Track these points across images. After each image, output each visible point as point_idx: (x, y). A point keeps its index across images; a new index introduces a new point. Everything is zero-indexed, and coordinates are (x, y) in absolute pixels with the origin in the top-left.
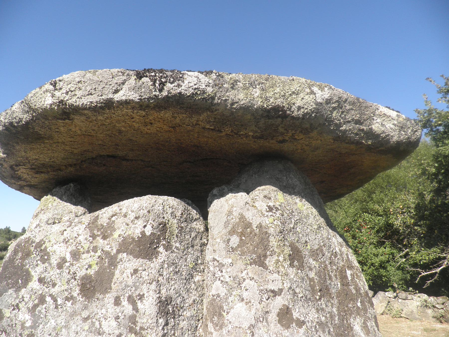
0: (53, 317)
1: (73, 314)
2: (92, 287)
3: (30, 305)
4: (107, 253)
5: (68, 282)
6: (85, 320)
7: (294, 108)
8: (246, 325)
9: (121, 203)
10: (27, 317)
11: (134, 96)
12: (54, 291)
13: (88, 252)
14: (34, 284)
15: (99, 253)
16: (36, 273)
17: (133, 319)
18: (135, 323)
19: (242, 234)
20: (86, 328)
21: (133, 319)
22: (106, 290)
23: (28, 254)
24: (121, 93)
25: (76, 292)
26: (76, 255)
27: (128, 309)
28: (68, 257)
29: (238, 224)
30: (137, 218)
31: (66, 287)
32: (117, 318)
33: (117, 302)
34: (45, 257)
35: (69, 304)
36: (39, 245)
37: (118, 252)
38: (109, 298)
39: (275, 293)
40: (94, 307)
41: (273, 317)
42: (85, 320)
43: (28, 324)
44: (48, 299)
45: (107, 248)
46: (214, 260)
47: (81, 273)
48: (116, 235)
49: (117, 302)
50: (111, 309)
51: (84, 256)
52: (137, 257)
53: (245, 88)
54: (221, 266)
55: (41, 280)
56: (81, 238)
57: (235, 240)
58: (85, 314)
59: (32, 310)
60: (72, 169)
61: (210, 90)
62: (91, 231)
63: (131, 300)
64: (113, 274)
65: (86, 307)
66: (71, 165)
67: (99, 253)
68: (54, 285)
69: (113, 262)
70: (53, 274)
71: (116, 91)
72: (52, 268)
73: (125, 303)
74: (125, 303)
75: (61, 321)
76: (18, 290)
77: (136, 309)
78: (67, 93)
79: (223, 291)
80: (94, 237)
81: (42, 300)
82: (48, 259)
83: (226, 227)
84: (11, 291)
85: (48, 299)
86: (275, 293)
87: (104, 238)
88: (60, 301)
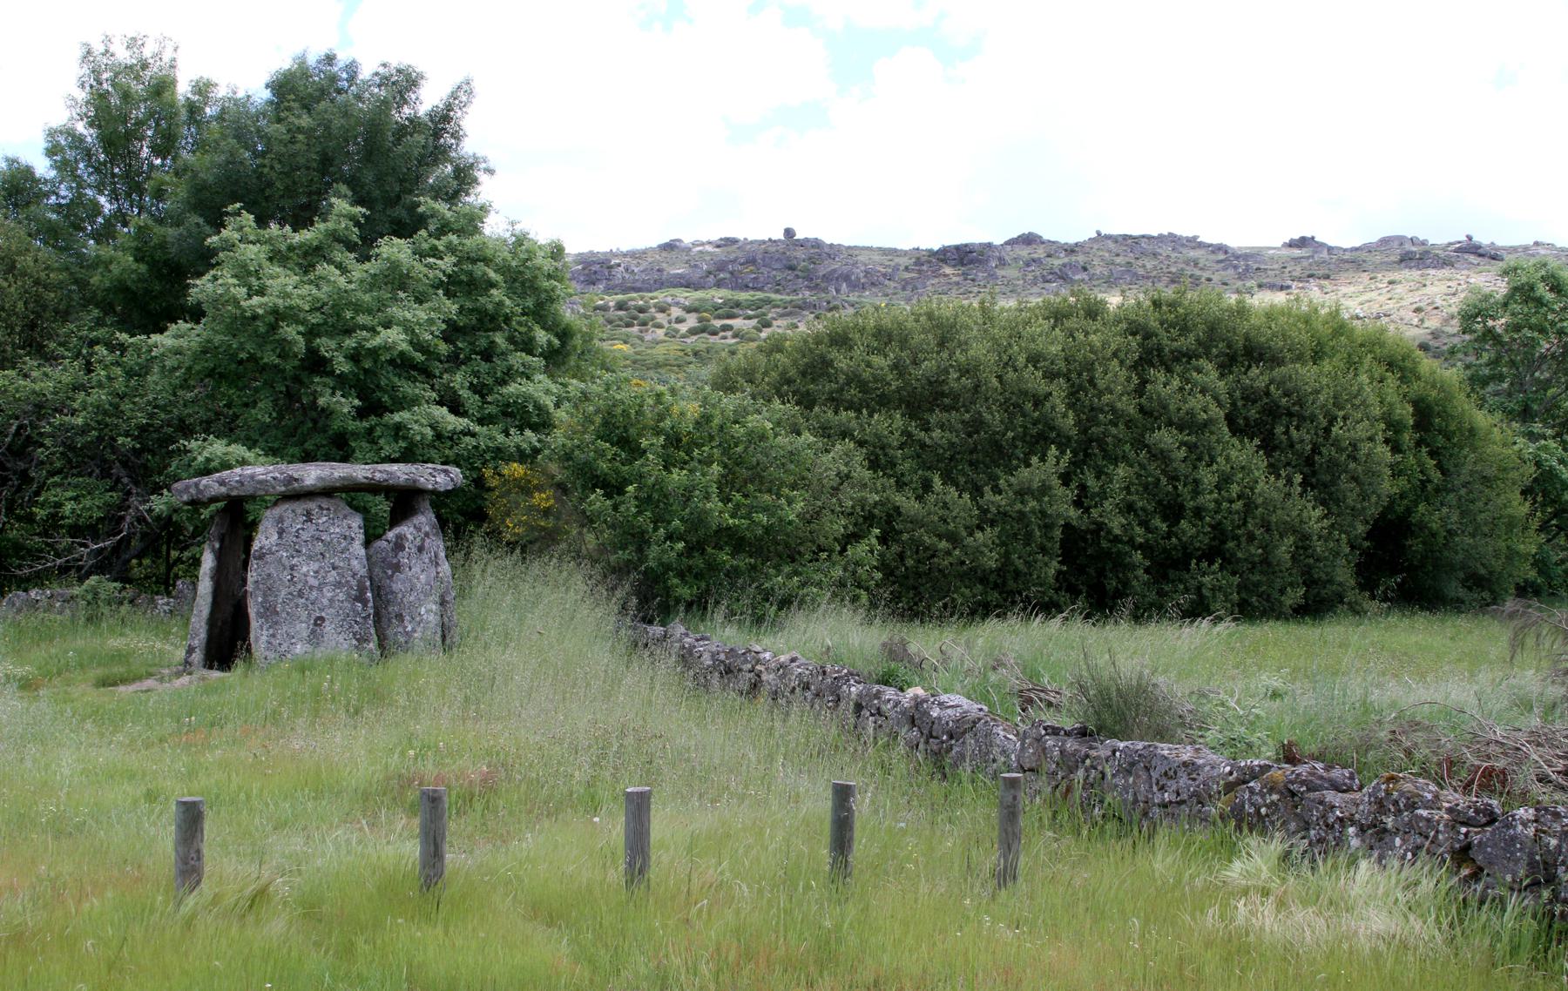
2: (421, 549)
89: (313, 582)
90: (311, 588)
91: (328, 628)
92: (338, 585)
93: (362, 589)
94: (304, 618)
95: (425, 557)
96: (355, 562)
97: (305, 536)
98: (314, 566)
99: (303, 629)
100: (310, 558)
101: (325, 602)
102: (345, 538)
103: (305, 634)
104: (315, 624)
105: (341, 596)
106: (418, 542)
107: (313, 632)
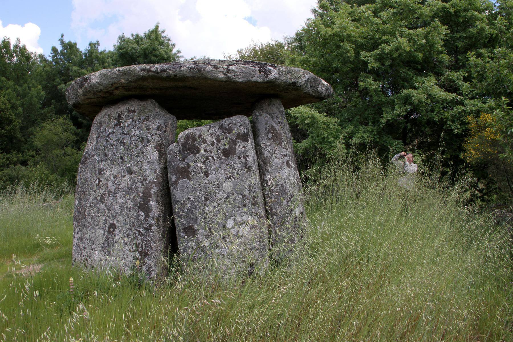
0: (214, 165)
1: (222, 163)
2: (228, 153)
3: (202, 160)
4: (232, 140)
5: (217, 151)
6: (227, 165)
7: (299, 83)
8: (279, 166)
9: (231, 118)
10: (202, 165)
11: (259, 80)
12: (213, 154)
13: (223, 139)
14: (202, 152)
15: (228, 139)
16: (202, 147)
17: (246, 164)
18: (246, 165)
19: (273, 133)
20: (228, 167)
21: (246, 164)
22: (235, 153)
23: (196, 140)
24: (254, 78)
25: (221, 155)
26: (218, 140)
27: (244, 160)
28: (215, 141)
29: (271, 128)
30: (241, 125)
31: (216, 153)
32: (240, 164)
33: (239, 158)
34: (204, 141)
35: (219, 160)
36: (200, 136)
37: (236, 139)
38: (236, 157)
39: (286, 156)
40: (229, 160)
41: (285, 164)
42: (227, 165)
43: (203, 168)
44: (210, 158)
45: (232, 138)
46: (263, 143)
47: (222, 147)
48: (234, 132)
49: (239, 158)
50: (237, 161)
51: (222, 141)
52: (243, 141)
53: (286, 75)
54: (266, 146)
55: (205, 151)
56: (218, 133)
57: (270, 135)
58: (227, 163)
59: (204, 163)
60: (158, 92)
61: (277, 76)
62: (223, 130)
63: (244, 157)
64: (236, 148)
65: (227, 161)
66: (157, 89)
67: (228, 139)
68: (211, 153)
69: (235, 143)
70: (209, 148)
71: (252, 77)
72: (209, 146)
73: (242, 158)
74: (242, 158)
75: (218, 166)
76: (195, 155)
77: (247, 160)
78: (234, 76)
79: (269, 155)
80: (225, 133)
81: (207, 158)
82: (206, 142)
83: (266, 130)
84: (191, 156)
85: (210, 158)
86: (286, 156)
87: (229, 133)
88: (215, 159)
89: (112, 187)
90: (110, 192)
91: (118, 236)
92: (129, 190)
93: (146, 197)
94: (101, 224)
95: (236, 162)
96: (146, 167)
97: (113, 139)
98: (115, 170)
99: (100, 233)
100: (113, 161)
101: (117, 207)
102: (142, 142)
103: (101, 241)
104: (109, 232)
105: (130, 204)
106: (224, 144)
107: (107, 240)
